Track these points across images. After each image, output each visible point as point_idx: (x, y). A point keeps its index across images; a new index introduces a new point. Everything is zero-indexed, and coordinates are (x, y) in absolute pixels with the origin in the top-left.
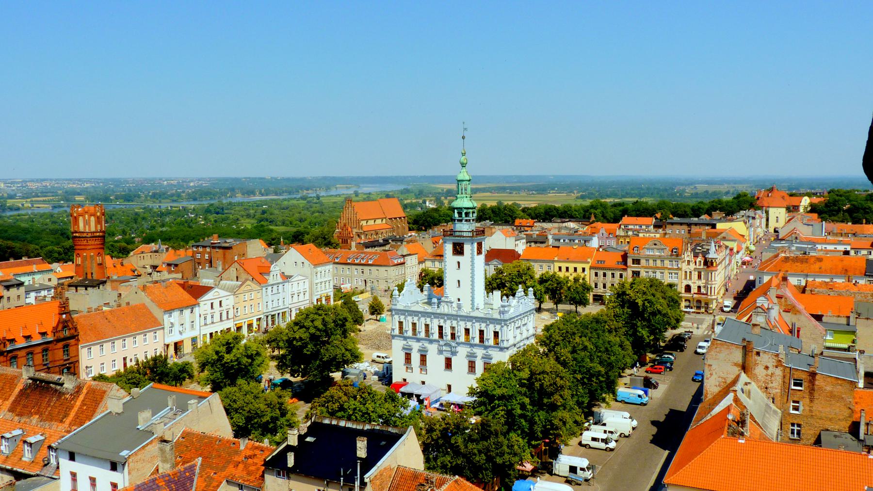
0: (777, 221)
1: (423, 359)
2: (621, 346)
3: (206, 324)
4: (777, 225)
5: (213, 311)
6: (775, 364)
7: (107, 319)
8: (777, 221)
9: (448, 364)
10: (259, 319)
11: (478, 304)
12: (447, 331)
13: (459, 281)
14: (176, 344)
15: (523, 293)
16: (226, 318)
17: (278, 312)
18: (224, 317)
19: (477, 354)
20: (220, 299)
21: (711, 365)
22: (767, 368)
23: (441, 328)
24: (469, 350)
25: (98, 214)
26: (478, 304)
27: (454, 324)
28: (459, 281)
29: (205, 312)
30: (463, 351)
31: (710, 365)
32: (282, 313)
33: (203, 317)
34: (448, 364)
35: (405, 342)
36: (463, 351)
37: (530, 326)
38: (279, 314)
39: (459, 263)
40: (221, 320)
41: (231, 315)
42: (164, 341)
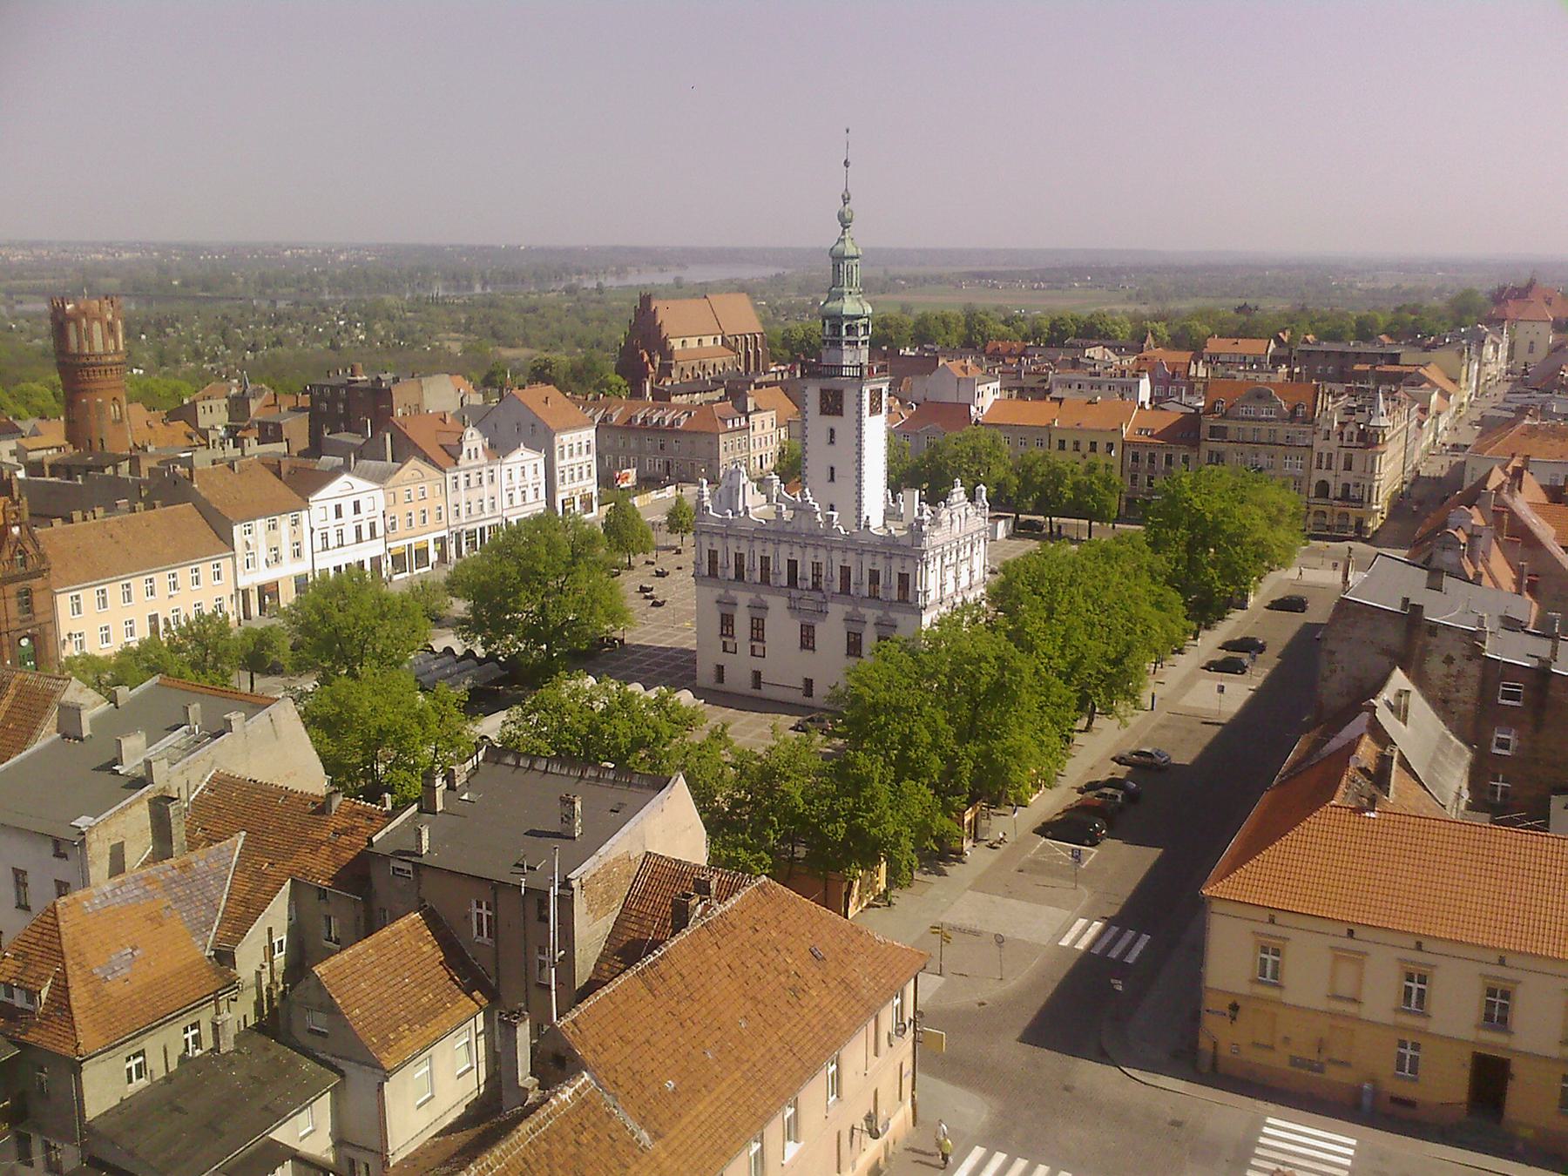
0: (1531, 351)
2: (1158, 605)
3: (326, 548)
4: (1530, 358)
5: (340, 521)
6: (1467, 653)
7: (111, 536)
8: (1531, 351)
9: (807, 640)
10: (442, 541)
11: (868, 518)
12: (804, 570)
13: (832, 468)
14: (262, 590)
15: (962, 496)
16: (369, 537)
17: (481, 524)
18: (366, 534)
19: (867, 618)
20: (356, 498)
21: (1334, 653)
22: (1449, 660)
23: (792, 565)
24: (849, 608)
25: (109, 317)
26: (868, 518)
27: (822, 556)
28: (832, 468)
29: (324, 524)
30: (837, 611)
31: (1332, 653)
32: (490, 527)
33: (317, 536)
34: (807, 640)
35: (722, 591)
36: (837, 611)
37: (979, 562)
38: (482, 529)
39: (832, 431)
40: (359, 539)
41: (380, 531)
42: (236, 583)
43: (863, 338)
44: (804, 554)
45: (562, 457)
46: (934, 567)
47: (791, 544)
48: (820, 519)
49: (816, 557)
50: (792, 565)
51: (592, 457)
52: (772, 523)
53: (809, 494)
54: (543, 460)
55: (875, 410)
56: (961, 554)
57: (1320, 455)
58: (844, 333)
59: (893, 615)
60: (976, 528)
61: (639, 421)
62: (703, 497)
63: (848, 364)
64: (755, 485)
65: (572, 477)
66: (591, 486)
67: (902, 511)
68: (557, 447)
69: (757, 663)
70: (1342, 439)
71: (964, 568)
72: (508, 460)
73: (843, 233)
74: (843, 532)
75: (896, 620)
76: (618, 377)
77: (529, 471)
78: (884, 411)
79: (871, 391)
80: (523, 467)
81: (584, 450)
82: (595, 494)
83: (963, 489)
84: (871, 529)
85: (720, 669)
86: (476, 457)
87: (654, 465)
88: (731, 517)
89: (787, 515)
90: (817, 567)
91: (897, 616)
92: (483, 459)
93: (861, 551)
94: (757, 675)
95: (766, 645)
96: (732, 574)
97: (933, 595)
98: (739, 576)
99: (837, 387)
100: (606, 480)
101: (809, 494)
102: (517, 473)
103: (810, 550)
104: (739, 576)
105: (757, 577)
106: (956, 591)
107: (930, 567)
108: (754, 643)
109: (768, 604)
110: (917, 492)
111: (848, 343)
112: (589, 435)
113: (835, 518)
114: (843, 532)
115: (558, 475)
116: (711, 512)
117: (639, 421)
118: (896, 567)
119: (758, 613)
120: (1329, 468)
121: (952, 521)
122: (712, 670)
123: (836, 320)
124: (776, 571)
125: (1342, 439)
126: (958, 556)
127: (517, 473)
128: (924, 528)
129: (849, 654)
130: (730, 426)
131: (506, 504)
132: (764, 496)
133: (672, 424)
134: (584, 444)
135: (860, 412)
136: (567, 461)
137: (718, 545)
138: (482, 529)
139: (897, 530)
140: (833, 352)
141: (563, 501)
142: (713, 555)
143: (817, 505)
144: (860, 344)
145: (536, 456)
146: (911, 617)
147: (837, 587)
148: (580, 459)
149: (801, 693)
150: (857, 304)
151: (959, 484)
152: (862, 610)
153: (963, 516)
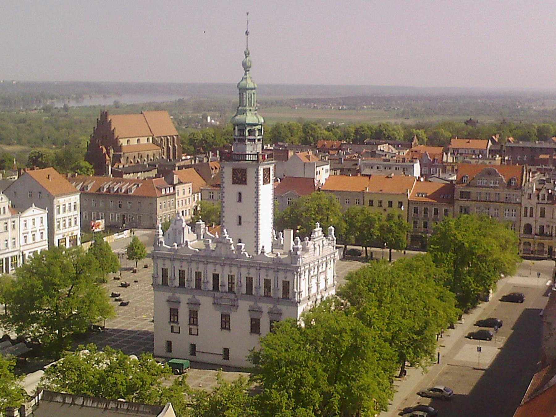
1: (193, 316)
2: (440, 298)
9: (225, 323)
11: (263, 247)
12: (224, 280)
13: (240, 218)
15: (321, 233)
17: (6, 256)
19: (263, 310)
23: (216, 277)
24: (251, 303)
26: (263, 247)
28: (240, 218)
30: (244, 305)
32: (12, 257)
34: (225, 323)
36: (244, 305)
37: (330, 273)
38: (7, 259)
39: (240, 194)
43: (259, 137)
44: (223, 270)
45: (59, 213)
46: (305, 276)
47: (215, 264)
48: (233, 248)
49: (231, 271)
50: (216, 277)
51: (78, 212)
52: (202, 251)
53: (226, 232)
54: (46, 215)
55: (266, 181)
56: (320, 269)
57: (526, 208)
58: (247, 134)
59: (279, 307)
60: (329, 253)
61: (105, 190)
62: (159, 235)
63: (250, 153)
64: (190, 228)
65: (65, 225)
66: (76, 231)
67: (282, 243)
68: (55, 206)
69: (193, 340)
70: (538, 198)
71: (322, 277)
72: (25, 214)
73: (246, 74)
74: (247, 256)
75: (281, 310)
76: (87, 162)
77: (38, 221)
78: (272, 182)
79: (264, 169)
80: (34, 219)
81: (73, 208)
82: (79, 236)
83: (321, 229)
84: (265, 254)
85: (169, 344)
86: (4, 213)
87: (116, 218)
88: (176, 247)
89: (212, 246)
90: (231, 278)
91: (282, 308)
92: (8, 214)
93: (259, 267)
94: (193, 347)
95: (199, 328)
96: (177, 283)
97: (304, 294)
98: (182, 284)
99: (243, 167)
100: (86, 227)
101: (226, 232)
102: (29, 223)
103: (227, 268)
104: (182, 284)
105: (193, 285)
106: (317, 291)
107: (302, 276)
108: (191, 327)
109: (201, 302)
110: (292, 231)
111: (249, 140)
112: (75, 198)
113: (243, 247)
114: (247, 256)
115: (56, 224)
116: (164, 245)
117: (105, 190)
118: (282, 277)
119: (194, 308)
120: (531, 216)
121: (315, 248)
122: (164, 344)
123: (242, 126)
124: (206, 281)
125: (538, 198)
126: (318, 270)
127: (29, 223)
128: (299, 253)
129: (251, 332)
130: (163, 193)
131: (22, 243)
132: (195, 235)
133: (127, 192)
134: (73, 204)
135: (257, 183)
136: (62, 215)
137: (168, 265)
138: (7, 259)
139: (281, 254)
140: (240, 146)
141: (59, 240)
142: (165, 272)
143: (231, 239)
144: (256, 141)
145: (42, 212)
146: (291, 308)
147: (244, 290)
148: (70, 214)
149: (221, 357)
150: (255, 117)
151: (319, 226)
152: (260, 305)
153: (321, 245)
